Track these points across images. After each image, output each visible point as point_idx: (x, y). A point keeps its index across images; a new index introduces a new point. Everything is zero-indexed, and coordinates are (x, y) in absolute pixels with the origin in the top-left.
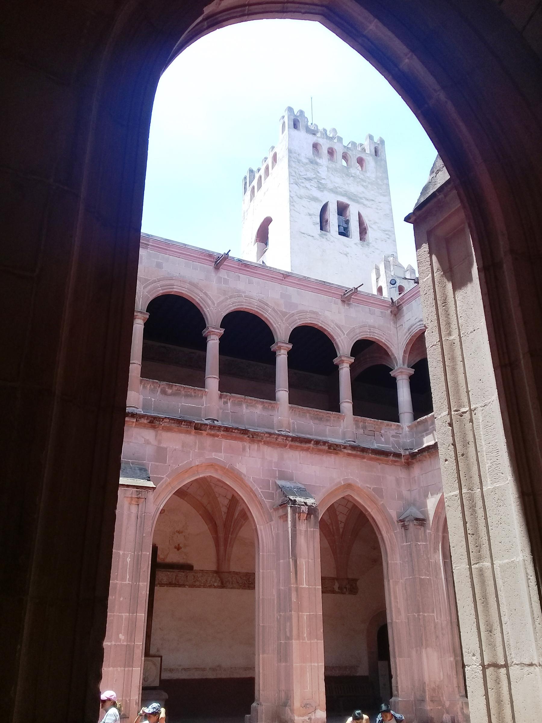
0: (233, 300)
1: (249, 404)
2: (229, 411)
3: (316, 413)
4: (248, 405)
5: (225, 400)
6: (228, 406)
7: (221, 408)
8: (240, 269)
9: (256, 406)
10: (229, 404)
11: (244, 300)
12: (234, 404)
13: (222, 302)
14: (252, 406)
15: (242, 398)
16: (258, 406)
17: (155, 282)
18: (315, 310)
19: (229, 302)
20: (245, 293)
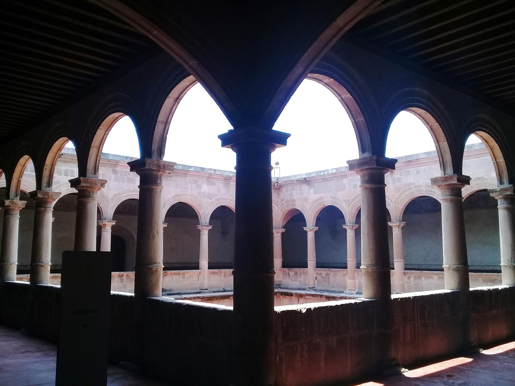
0: (406, 194)
1: (427, 277)
2: (413, 284)
3: (487, 277)
4: (426, 277)
5: (409, 275)
6: (411, 280)
7: (406, 283)
8: (408, 165)
9: (433, 277)
10: (412, 278)
11: (415, 190)
12: (415, 278)
13: (398, 198)
14: (429, 278)
15: (420, 273)
16: (434, 276)
17: (354, 200)
18: (479, 176)
19: (403, 196)
20: (414, 184)
